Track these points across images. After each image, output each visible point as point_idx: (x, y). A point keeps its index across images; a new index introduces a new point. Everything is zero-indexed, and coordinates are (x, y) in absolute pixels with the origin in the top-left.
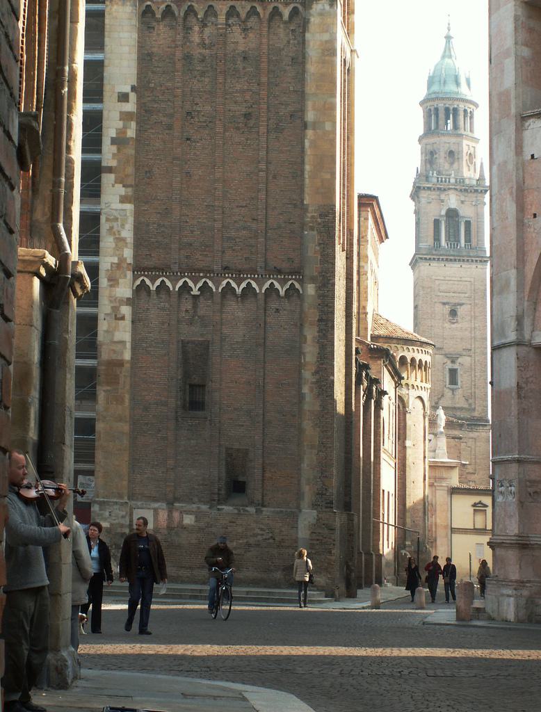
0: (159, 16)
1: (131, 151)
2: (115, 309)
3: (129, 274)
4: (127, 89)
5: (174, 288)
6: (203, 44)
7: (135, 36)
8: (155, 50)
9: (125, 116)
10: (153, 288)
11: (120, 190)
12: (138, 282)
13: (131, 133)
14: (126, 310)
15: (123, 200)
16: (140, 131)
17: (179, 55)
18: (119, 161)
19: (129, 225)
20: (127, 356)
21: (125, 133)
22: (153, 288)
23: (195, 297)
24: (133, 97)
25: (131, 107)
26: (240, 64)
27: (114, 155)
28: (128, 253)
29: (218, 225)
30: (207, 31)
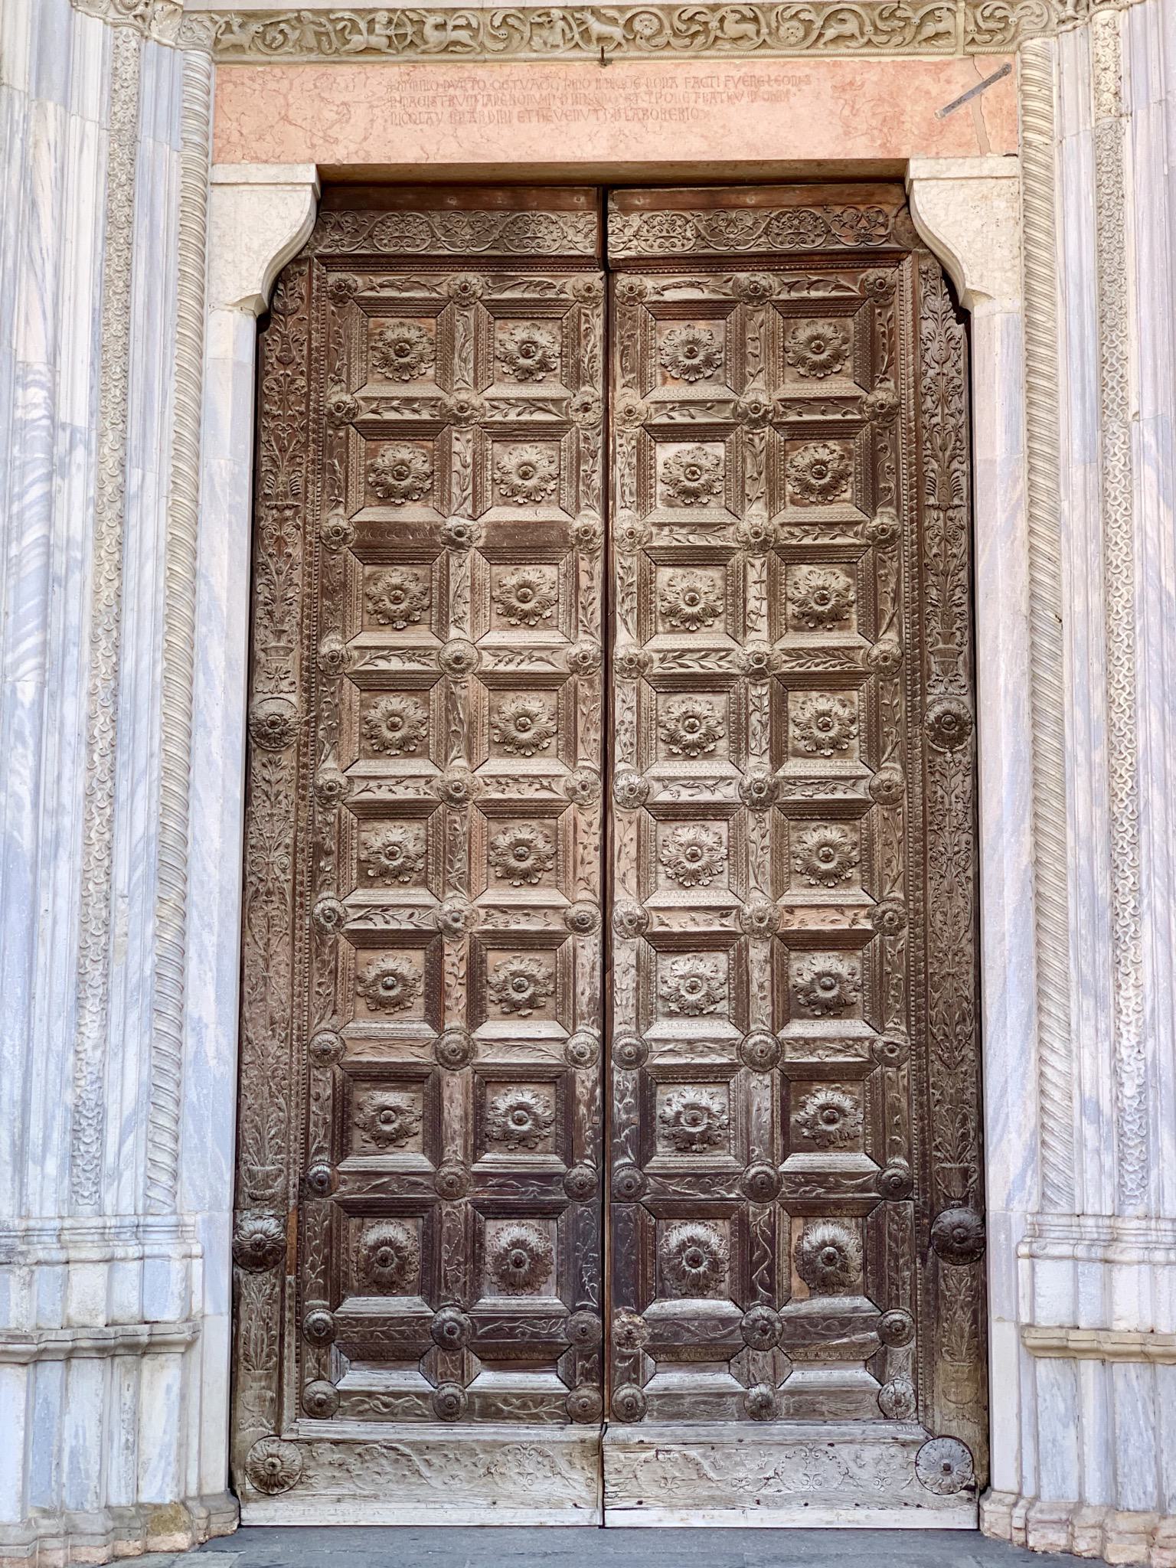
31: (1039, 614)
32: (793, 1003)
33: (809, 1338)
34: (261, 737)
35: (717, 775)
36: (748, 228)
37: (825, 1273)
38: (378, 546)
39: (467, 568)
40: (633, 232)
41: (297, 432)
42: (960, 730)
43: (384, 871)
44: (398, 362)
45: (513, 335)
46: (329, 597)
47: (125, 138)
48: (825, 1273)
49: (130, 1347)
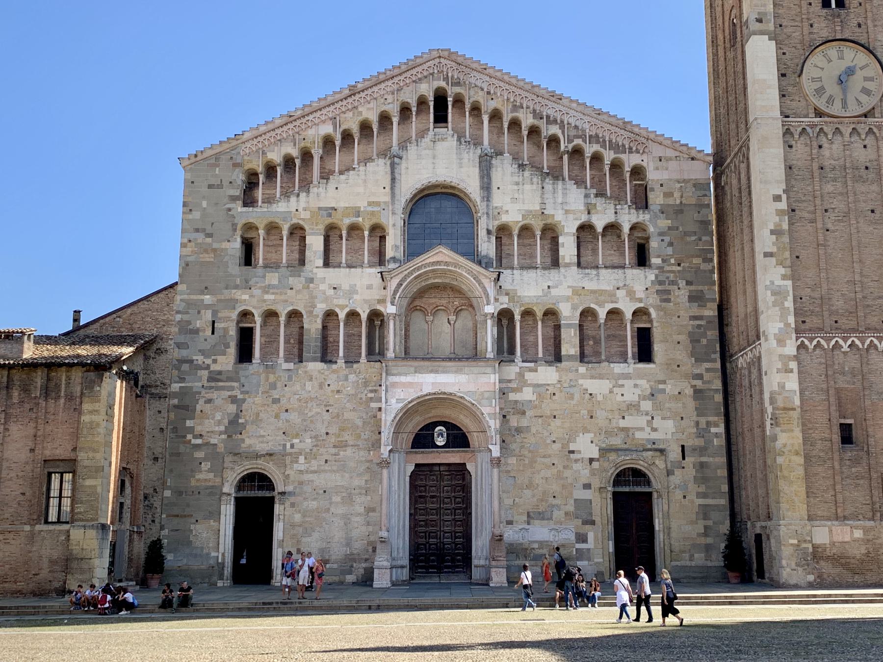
0: (797, 136)
1: (786, 239)
2: (785, 365)
3: (794, 336)
4: (781, 192)
5: (828, 346)
6: (832, 157)
7: (782, 151)
8: (794, 162)
9: (780, 213)
10: (811, 347)
11: (782, 271)
12: (799, 342)
13: (785, 226)
14: (793, 365)
15: (784, 277)
16: (791, 224)
17: (815, 166)
18: (778, 248)
19: (790, 298)
20: (797, 402)
21: (780, 225)
22: (811, 347)
23: (845, 353)
24: (784, 197)
25: (783, 205)
26: (863, 172)
27: (773, 244)
28: (791, 319)
29: (859, 296)
30: (834, 147)
31: (477, 504)
32: (456, 538)
33: (458, 567)
34: (410, 514)
35: (449, 518)
36: (452, 468)
37: (459, 561)
38: (421, 497)
39: (428, 499)
40: (442, 468)
41: (413, 486)
42: (471, 513)
43: (421, 526)
44: (421, 480)
45: (432, 477)
46: (416, 502)
47: (399, 464)
48: (459, 561)
49: (402, 567)
